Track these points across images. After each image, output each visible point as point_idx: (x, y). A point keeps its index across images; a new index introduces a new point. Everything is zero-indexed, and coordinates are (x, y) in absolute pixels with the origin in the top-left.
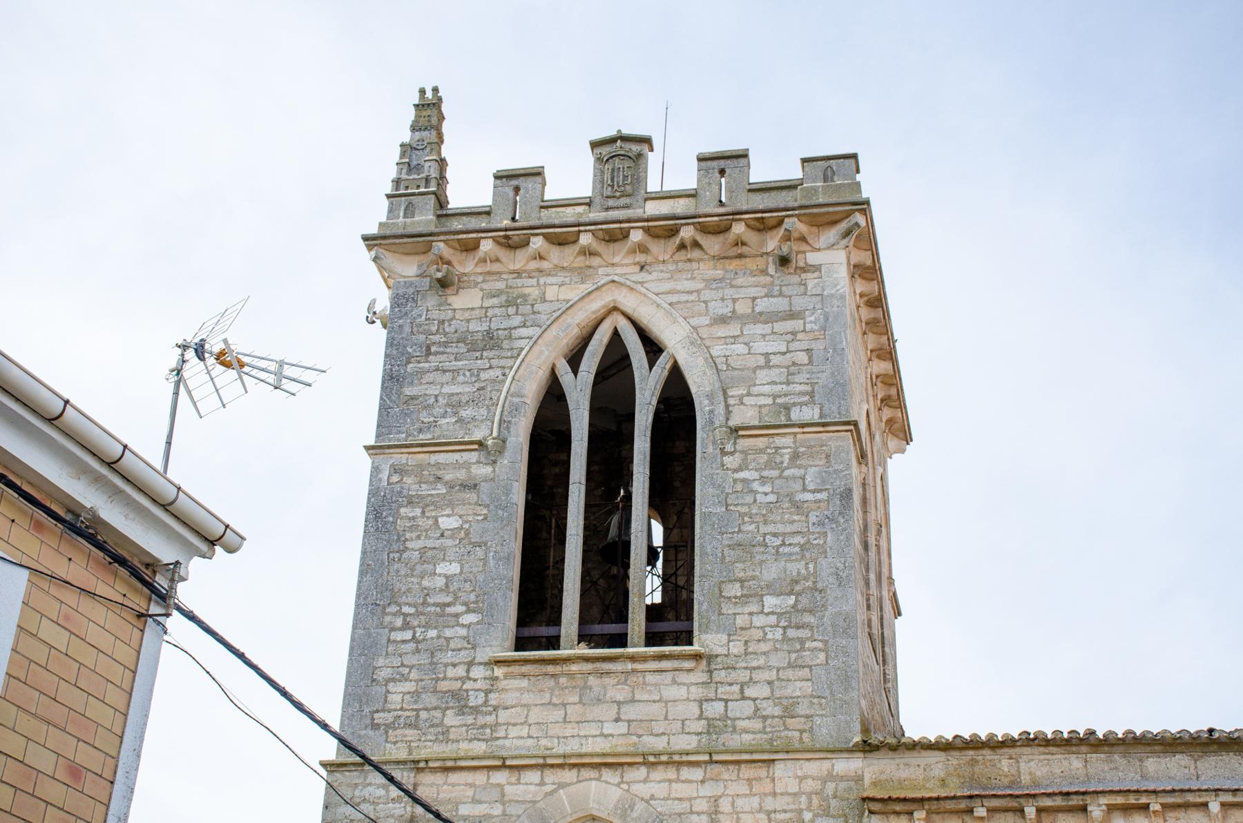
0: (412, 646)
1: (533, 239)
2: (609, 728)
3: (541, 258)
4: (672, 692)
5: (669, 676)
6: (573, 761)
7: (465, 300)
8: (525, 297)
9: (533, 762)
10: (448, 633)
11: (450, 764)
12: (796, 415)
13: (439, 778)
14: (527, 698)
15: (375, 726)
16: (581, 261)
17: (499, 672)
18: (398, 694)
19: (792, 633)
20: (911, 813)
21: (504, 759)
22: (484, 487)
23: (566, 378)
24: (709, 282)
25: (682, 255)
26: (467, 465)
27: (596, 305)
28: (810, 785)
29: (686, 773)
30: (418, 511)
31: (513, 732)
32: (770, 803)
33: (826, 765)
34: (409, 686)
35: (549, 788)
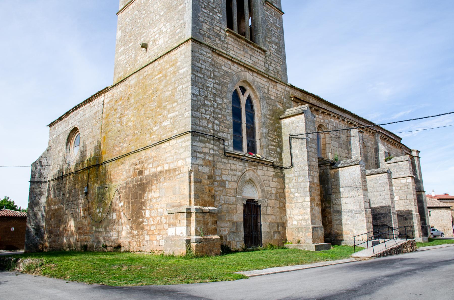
0: (206, 15)
4: (260, 58)
5: (259, 54)
10: (215, 16)
11: (221, 53)
12: (274, 4)
14: (233, 44)
15: (200, 34)
17: (228, 34)
18: (205, 27)
19: (277, 55)
20: (297, 103)
21: (232, 58)
28: (282, 91)
29: (264, 79)
31: (231, 52)
33: (285, 87)
34: (207, 26)
35: (240, 70)
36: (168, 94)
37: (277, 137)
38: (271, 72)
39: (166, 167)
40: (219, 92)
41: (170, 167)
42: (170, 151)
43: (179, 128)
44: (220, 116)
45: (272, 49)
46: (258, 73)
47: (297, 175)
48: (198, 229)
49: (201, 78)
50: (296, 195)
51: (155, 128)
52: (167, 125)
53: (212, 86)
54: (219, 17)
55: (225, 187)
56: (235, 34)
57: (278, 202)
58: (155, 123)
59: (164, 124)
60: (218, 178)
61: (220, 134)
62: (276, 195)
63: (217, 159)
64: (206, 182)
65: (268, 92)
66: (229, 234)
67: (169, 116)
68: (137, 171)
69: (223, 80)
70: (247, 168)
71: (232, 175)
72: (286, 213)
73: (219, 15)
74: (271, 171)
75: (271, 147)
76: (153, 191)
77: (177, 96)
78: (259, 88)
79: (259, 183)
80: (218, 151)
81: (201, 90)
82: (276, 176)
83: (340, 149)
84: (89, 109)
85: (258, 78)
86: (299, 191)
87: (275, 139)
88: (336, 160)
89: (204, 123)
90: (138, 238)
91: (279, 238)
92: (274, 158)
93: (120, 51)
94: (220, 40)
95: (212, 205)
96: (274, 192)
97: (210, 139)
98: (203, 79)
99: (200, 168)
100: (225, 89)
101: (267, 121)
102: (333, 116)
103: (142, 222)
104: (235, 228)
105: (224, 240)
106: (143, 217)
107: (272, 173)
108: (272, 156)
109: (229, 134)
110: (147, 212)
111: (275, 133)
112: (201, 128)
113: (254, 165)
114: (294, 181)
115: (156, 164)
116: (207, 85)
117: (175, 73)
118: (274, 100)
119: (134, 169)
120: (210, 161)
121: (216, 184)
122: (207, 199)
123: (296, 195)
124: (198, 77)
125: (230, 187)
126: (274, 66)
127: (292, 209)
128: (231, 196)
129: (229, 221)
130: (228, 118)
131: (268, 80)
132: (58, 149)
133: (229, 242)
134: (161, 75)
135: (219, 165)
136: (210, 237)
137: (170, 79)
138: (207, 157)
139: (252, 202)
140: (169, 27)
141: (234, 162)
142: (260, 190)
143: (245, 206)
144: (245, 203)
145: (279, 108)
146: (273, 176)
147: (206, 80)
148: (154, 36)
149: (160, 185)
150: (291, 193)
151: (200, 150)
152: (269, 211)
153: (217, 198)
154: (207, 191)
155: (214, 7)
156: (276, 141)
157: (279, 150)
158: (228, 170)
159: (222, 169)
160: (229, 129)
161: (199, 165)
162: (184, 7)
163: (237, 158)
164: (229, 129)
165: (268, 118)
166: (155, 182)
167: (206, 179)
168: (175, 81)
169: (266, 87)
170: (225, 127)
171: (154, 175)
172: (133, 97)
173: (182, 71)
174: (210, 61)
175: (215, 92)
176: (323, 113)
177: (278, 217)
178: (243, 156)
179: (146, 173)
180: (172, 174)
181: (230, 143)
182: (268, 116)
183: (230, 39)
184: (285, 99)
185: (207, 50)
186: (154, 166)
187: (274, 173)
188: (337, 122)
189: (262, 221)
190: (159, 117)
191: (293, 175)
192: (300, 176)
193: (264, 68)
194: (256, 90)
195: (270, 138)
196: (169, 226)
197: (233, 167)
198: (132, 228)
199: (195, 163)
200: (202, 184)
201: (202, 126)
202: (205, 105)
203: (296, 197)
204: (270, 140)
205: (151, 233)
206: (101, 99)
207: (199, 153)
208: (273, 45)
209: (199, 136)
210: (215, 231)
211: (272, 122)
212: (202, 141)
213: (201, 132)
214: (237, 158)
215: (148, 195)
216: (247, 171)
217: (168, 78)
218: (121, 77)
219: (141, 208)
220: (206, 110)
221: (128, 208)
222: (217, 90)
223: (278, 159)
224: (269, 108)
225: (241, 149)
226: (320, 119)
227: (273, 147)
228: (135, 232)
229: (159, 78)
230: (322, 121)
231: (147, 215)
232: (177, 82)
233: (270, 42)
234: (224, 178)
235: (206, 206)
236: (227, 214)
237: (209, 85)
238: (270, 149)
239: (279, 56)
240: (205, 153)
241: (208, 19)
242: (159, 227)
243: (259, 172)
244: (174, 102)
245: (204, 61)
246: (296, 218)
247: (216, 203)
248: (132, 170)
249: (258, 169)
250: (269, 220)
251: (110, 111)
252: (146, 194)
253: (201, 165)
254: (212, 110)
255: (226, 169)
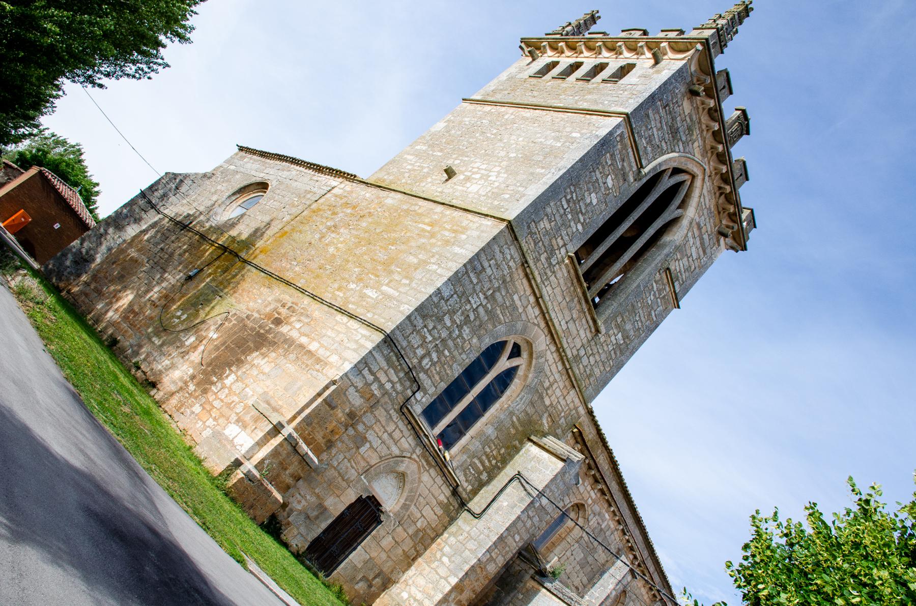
0: (562, 211)
1: (717, 124)
2: (563, 323)
3: (708, 130)
4: (582, 332)
5: (586, 326)
6: (550, 323)
7: (687, 106)
8: (692, 134)
9: (544, 308)
10: (572, 223)
11: (531, 276)
12: (676, 284)
13: (522, 274)
14: (562, 281)
15: (529, 227)
16: (708, 147)
17: (567, 261)
18: (545, 224)
19: (612, 352)
20: (577, 442)
22: (626, 185)
23: (666, 177)
24: (710, 209)
25: (716, 189)
26: (631, 167)
27: (696, 170)
28: (571, 406)
30: (609, 163)
31: (549, 288)
32: (561, 399)
34: (548, 227)
35: (536, 322)
36: (413, 260)
37: (499, 458)
38: (581, 366)
39: (313, 347)
40: (477, 323)
41: (316, 351)
42: (339, 332)
43: (379, 315)
44: (446, 353)
45: (613, 338)
46: (558, 350)
47: (472, 534)
48: (267, 462)
49: (471, 282)
50: (445, 559)
51: (352, 286)
52: (369, 297)
53: (475, 306)
54: (577, 230)
55: (358, 448)
56: (576, 271)
57: (412, 544)
58: (360, 279)
59: (369, 292)
60: (360, 428)
61: (422, 376)
62: (418, 530)
63: (386, 403)
64: (340, 415)
65: (548, 388)
66: (300, 512)
67: (384, 288)
68: (277, 315)
69: (499, 312)
70: (414, 456)
71: (383, 442)
72: (407, 570)
73: (580, 227)
74: (444, 494)
75: (477, 462)
76: (266, 359)
77: (418, 275)
78: (540, 371)
79: (411, 491)
80: (397, 393)
81: (455, 296)
82: (445, 507)
83: (578, 567)
84: (306, 179)
85: (551, 357)
86: (453, 559)
87: (495, 458)
88: (553, 573)
89: (416, 341)
90: (186, 398)
91: (361, 592)
92: (467, 481)
93: (418, 147)
94: (548, 259)
95: (318, 451)
96: (419, 524)
97: (403, 369)
98: (472, 286)
99: (352, 390)
100: (490, 326)
101: (507, 423)
102: (614, 511)
103: (213, 383)
104: (315, 513)
105: (285, 514)
106: (220, 378)
107: (442, 498)
108: (465, 475)
109: (436, 387)
110: (232, 377)
111: (503, 451)
112: (404, 344)
113: (427, 461)
114: (461, 538)
115: (306, 329)
116: (470, 299)
117: (447, 242)
118: (546, 407)
119: (275, 310)
120: (373, 395)
121: (351, 431)
122: (319, 437)
123: (445, 559)
124: (469, 276)
125: (366, 456)
126: (592, 363)
127: (420, 574)
128: (353, 468)
129: (318, 496)
130: (455, 365)
131: (565, 372)
132: (219, 187)
133: (289, 524)
134: (429, 228)
135: (380, 413)
136: (270, 487)
137: (433, 245)
138: (374, 387)
139: (376, 506)
140: (501, 180)
141: (404, 428)
142: (402, 501)
143: (360, 500)
144: (364, 497)
145: (542, 424)
146: (440, 504)
147: (475, 291)
148: (474, 173)
149: (282, 361)
150: (441, 550)
151: (375, 368)
152: (387, 542)
153: (334, 451)
154: (330, 428)
155: (584, 211)
156: (494, 462)
157: (484, 477)
158: (386, 431)
159: (379, 421)
160: (442, 380)
161: (353, 385)
162: (544, 175)
163: (413, 428)
164: (442, 380)
165: (513, 422)
166: (281, 351)
167: (343, 412)
168: (437, 253)
169: (551, 379)
170: (439, 373)
171: (289, 342)
172: (370, 220)
173: (457, 250)
174: (505, 273)
175: (472, 317)
176: (602, 492)
177: (390, 563)
178: (425, 435)
179: (284, 329)
180: (309, 362)
181: (424, 400)
182: (515, 419)
183: (565, 271)
184: (563, 420)
185: (517, 256)
186: (302, 330)
187: (446, 501)
188: (612, 526)
189: (363, 544)
190: (373, 277)
191: (468, 528)
192: (475, 540)
193: (575, 352)
194: (533, 369)
195: (488, 450)
196: (238, 421)
197: (397, 435)
198: (193, 377)
199: (351, 377)
200: (332, 412)
201: (409, 342)
202: (440, 320)
203: (442, 563)
204: (485, 453)
205: (208, 407)
206: (334, 181)
207: (370, 370)
208: (620, 335)
209: (392, 350)
210: (284, 489)
211: (513, 431)
212: (388, 360)
213: (399, 348)
214: (413, 428)
215: (255, 358)
216: (410, 458)
217: (433, 241)
218: (384, 181)
219: (230, 365)
220: (434, 328)
221: (217, 348)
222: (477, 317)
223: (470, 487)
224: (528, 409)
225: (433, 423)
226: (590, 496)
227: (479, 465)
228: (192, 387)
229: (423, 230)
230: (590, 501)
231: (228, 382)
232: (437, 256)
233: (618, 327)
234: (370, 436)
235: (308, 445)
236: (325, 485)
237: (473, 302)
238: (473, 465)
239: (613, 356)
240: (377, 379)
241: (558, 218)
242: (225, 410)
243: (425, 478)
244: (406, 277)
245: (498, 266)
246: (413, 590)
247: (325, 456)
248: (272, 307)
249: (428, 471)
250: (374, 554)
251: (326, 208)
252: (255, 354)
253: (356, 387)
254: (444, 334)
255: (384, 427)
